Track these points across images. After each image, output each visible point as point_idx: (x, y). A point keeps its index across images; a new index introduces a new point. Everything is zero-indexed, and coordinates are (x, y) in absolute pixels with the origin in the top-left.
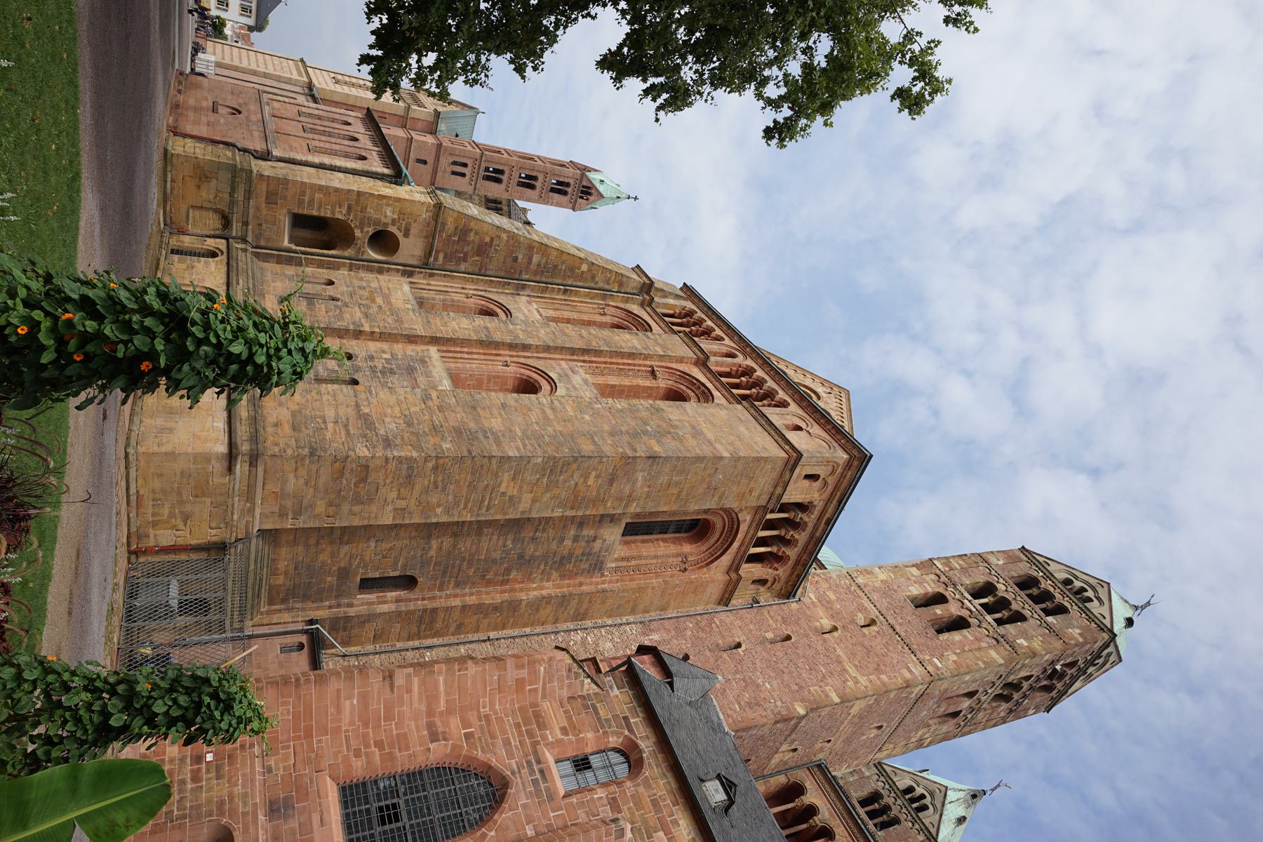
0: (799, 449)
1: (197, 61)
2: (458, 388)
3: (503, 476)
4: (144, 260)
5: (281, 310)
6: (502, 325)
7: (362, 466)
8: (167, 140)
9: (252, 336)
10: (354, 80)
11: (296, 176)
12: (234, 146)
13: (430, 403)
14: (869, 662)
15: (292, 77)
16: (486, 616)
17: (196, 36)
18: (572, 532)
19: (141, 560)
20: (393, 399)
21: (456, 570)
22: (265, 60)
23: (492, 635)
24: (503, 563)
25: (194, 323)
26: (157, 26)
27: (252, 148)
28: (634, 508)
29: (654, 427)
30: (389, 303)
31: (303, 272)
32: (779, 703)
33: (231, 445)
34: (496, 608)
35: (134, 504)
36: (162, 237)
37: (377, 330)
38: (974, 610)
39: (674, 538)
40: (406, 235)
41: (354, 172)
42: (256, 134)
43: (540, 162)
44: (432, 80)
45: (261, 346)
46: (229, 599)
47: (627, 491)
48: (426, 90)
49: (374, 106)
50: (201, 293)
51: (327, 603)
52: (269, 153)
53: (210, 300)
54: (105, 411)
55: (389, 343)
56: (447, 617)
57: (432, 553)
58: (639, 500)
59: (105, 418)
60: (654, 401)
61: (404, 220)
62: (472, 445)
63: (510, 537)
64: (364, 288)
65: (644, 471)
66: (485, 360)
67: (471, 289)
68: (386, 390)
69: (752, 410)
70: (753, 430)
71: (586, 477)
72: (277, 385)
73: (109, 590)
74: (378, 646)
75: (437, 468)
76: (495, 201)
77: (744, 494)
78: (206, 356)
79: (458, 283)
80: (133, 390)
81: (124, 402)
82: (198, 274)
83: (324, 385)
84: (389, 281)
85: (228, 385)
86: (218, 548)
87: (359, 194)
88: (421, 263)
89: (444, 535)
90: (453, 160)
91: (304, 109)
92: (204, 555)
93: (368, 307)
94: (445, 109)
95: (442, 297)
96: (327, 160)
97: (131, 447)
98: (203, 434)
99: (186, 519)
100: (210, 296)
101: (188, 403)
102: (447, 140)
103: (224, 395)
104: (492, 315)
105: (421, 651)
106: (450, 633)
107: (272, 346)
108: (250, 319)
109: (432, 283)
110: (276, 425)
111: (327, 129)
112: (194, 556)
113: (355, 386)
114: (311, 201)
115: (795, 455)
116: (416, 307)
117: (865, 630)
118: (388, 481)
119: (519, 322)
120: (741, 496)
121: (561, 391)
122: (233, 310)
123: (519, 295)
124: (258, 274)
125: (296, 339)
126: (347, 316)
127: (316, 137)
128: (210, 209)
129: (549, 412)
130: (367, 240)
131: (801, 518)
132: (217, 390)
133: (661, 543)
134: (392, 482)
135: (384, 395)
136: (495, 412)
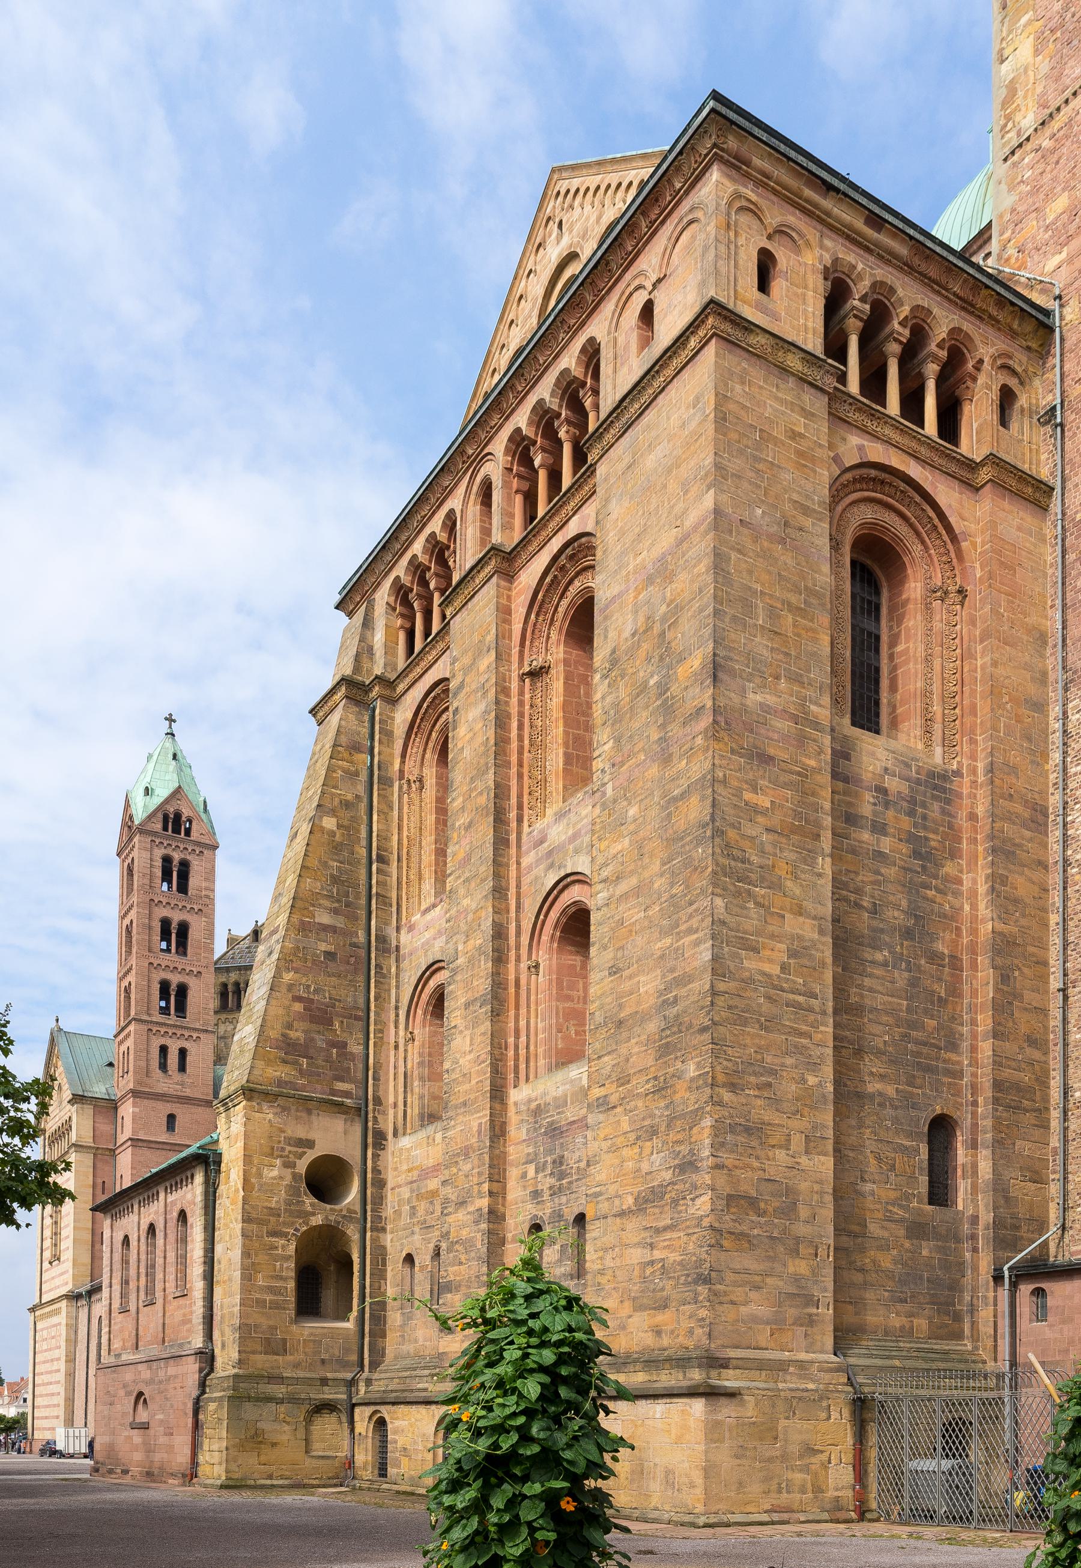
0: (697, 309)
1: (71, 1451)
2: (584, 1052)
3: (749, 970)
4: (401, 1510)
5: (463, 1330)
6: (458, 978)
7: (728, 1205)
8: (206, 1486)
9: (510, 1369)
10: (48, 1233)
11: (232, 1314)
12: (197, 1401)
13: (614, 1099)
15: (64, 1322)
16: (1017, 996)
17: (31, 1452)
18: (866, 836)
19: (874, 1505)
20: (608, 1159)
21: (925, 1050)
22: (44, 1362)
23: (1055, 983)
24: (919, 967)
25: (496, 1446)
26: (27, 1501)
27: (197, 1376)
28: (822, 711)
29: (650, 669)
30: (436, 1169)
31: (395, 1299)
33: (692, 1393)
34: (1004, 977)
35: (785, 1516)
36: (361, 1489)
37: (486, 1187)
39: (891, 619)
40: (310, 1144)
41: (210, 1228)
42: (172, 1370)
43: (133, 915)
44: (17, 1110)
45: (526, 1356)
46: (948, 1392)
47: (783, 725)
48: (38, 1118)
49: (86, 1200)
50: (445, 1438)
51: (968, 1255)
52: (199, 1353)
53: (456, 1426)
54: (640, 1552)
55: (508, 1168)
56: (1013, 1064)
57: (890, 1090)
58: (804, 699)
59: (651, 1552)
60: (596, 671)
61: (283, 1149)
62: (691, 1026)
63: (868, 954)
64: (413, 1208)
65: (744, 690)
66: (528, 1006)
67: (396, 1033)
68: (592, 1170)
69: (609, 437)
70: (653, 434)
71: (755, 810)
72: (590, 1332)
73: (919, 1544)
74: (1052, 1177)
75: (733, 1085)
76: (223, 994)
77: (800, 454)
78: (549, 1429)
79: (388, 1056)
80: (607, 1520)
81: (626, 1530)
82: (415, 1442)
83: (587, 1265)
84: (396, 1169)
85: (594, 1399)
86: (862, 1408)
87: (247, 1219)
88: (357, 1119)
89: (859, 1071)
90: (158, 1070)
91: (116, 1304)
92: (872, 1429)
93: (446, 1201)
94: (65, 1087)
95: (416, 1083)
96: (196, 1270)
97: (696, 1520)
98: (674, 1431)
99: (811, 1451)
100: (450, 1426)
101: (623, 1453)
102: (122, 1083)
103: (611, 1405)
104: (442, 994)
105: (1071, 1106)
106: (1043, 1058)
107: (525, 1340)
108: (483, 1373)
109: (391, 1100)
110: (658, 1333)
111: (143, 1270)
112: (873, 1439)
113: (588, 1218)
114: (271, 1290)
115: (710, 321)
116: (439, 1125)
118: (756, 1164)
119: (451, 945)
120: (805, 459)
121: (582, 864)
122: (469, 1395)
123: (398, 948)
124: (407, 1362)
125: (511, 1308)
126: (464, 1233)
127: (159, 1286)
128: (307, 1431)
129: (623, 887)
130: (328, 1206)
131: (863, 299)
132: (602, 1414)
133: (900, 648)
134: (757, 1158)
135: (600, 1174)
136: (627, 986)
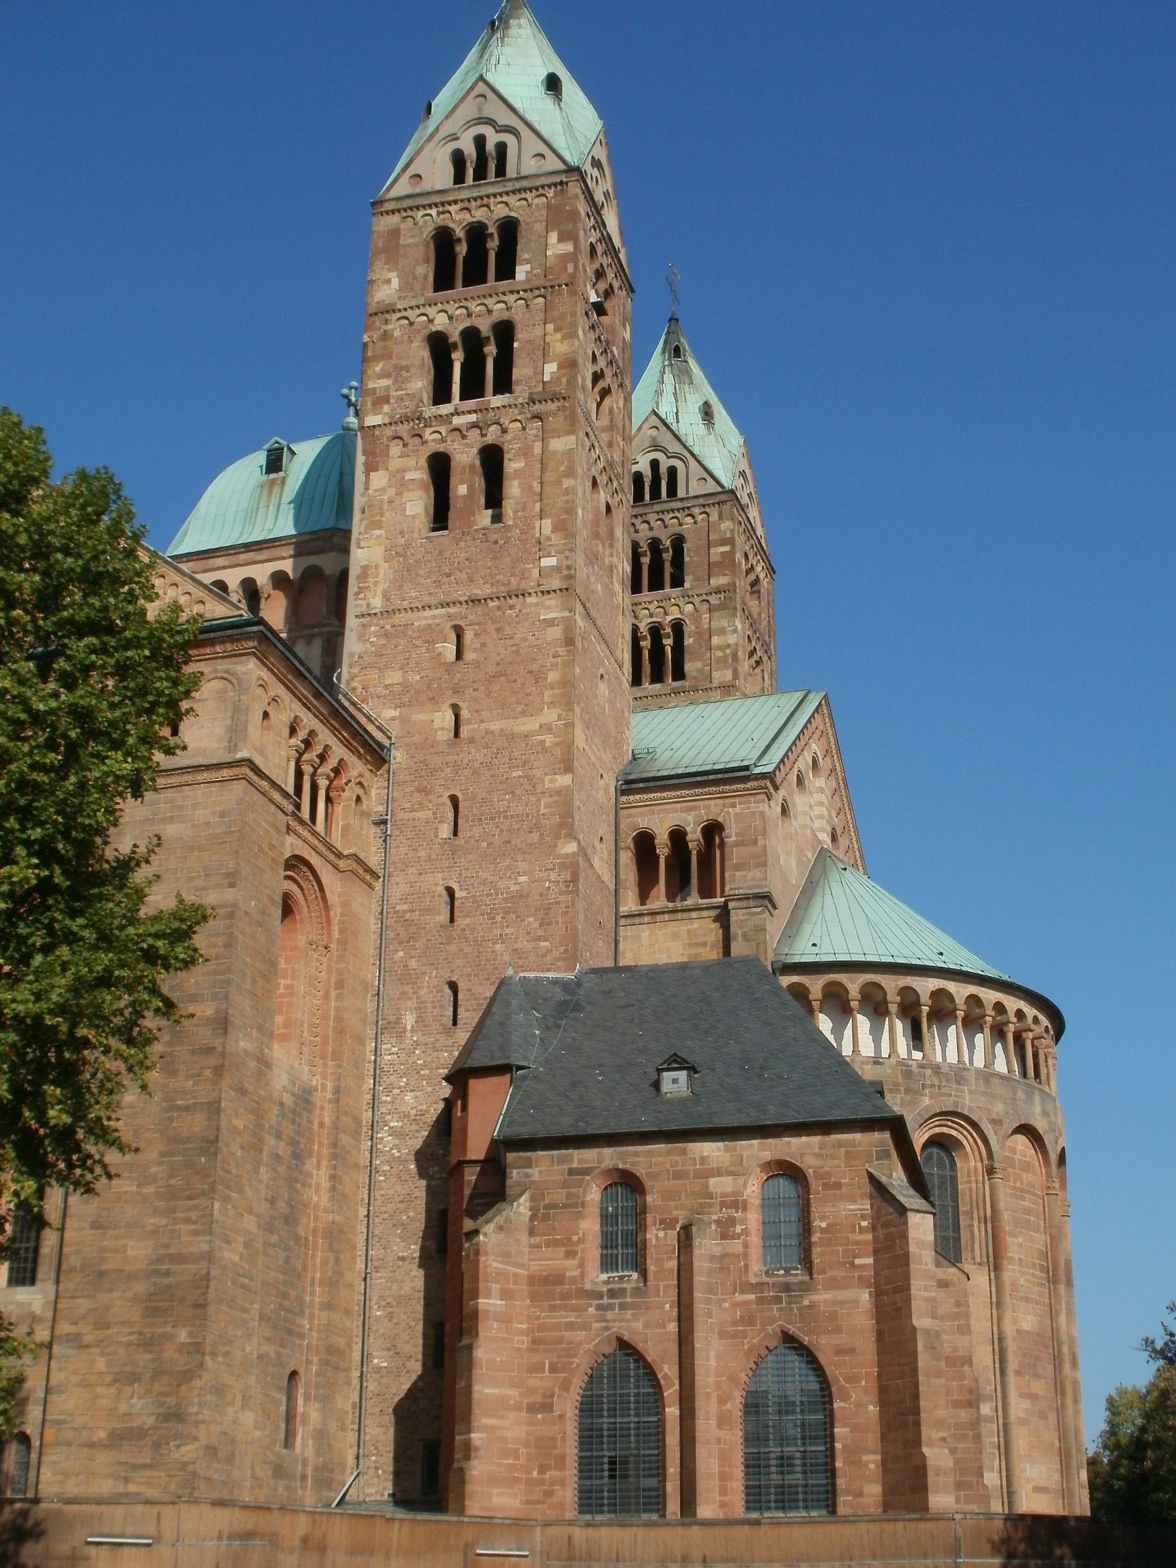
14: (523, 684)
32: (553, 876)
38: (473, 418)
117: (469, 656)
